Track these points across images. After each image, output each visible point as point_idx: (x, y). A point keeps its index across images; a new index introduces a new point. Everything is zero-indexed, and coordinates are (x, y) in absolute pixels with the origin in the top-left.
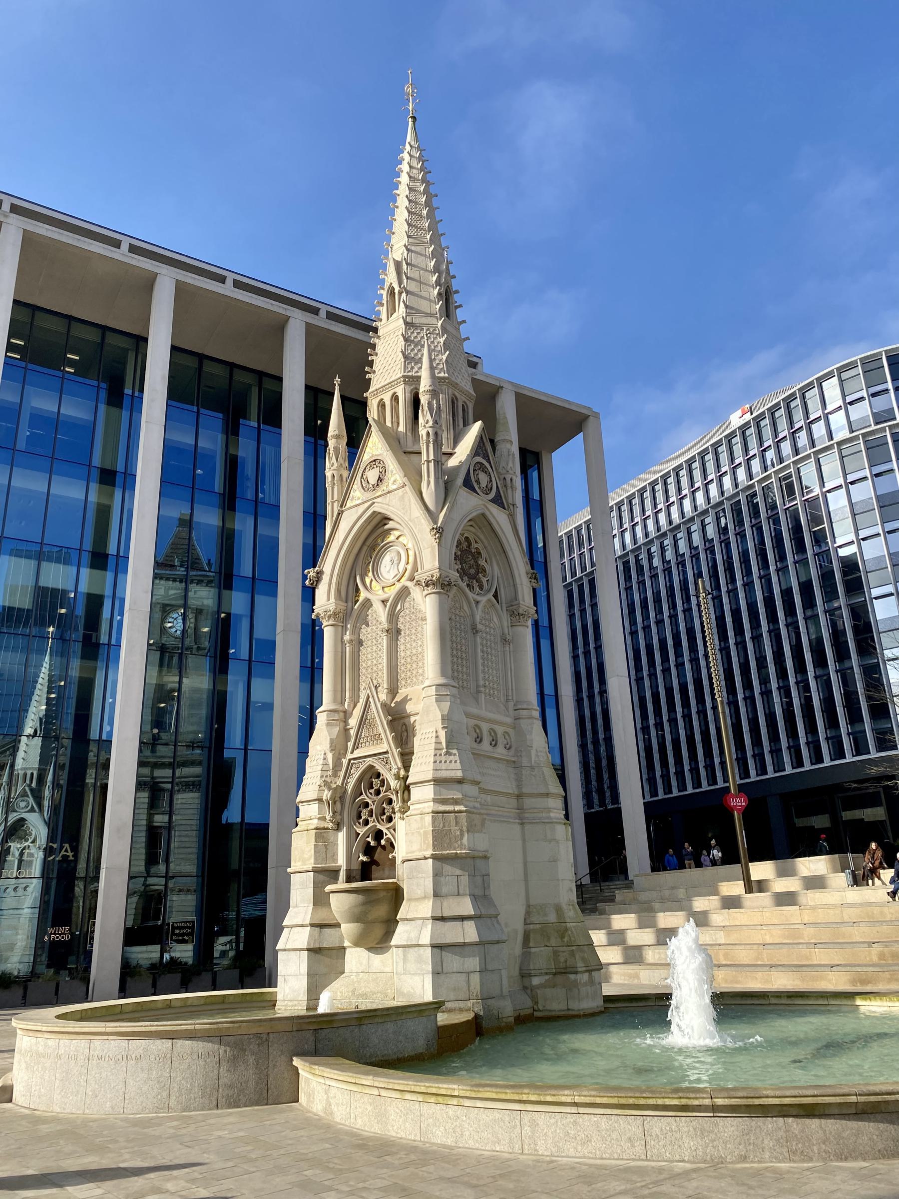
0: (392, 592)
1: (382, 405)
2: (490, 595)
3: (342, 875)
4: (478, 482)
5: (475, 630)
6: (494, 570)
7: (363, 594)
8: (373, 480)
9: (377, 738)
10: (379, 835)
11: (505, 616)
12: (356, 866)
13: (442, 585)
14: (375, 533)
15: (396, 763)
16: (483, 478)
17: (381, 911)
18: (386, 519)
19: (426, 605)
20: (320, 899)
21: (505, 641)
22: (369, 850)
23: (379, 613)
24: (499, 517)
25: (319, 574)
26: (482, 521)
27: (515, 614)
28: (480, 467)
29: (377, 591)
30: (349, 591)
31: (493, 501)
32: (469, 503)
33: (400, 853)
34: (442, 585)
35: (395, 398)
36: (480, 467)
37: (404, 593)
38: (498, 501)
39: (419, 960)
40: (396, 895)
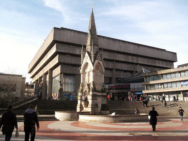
0: (88, 71)
5: (97, 75)
7: (86, 71)
8: (86, 58)
10: (87, 97)
13: (93, 71)
14: (87, 64)
16: (99, 58)
17: (86, 104)
18: (88, 63)
19: (91, 74)
21: (101, 76)
22: (86, 98)
23: (87, 73)
24: (101, 62)
25: (81, 68)
26: (99, 63)
27: (102, 73)
29: (87, 70)
31: (100, 60)
33: (88, 99)
34: (93, 71)
37: (90, 71)
40: (88, 102)
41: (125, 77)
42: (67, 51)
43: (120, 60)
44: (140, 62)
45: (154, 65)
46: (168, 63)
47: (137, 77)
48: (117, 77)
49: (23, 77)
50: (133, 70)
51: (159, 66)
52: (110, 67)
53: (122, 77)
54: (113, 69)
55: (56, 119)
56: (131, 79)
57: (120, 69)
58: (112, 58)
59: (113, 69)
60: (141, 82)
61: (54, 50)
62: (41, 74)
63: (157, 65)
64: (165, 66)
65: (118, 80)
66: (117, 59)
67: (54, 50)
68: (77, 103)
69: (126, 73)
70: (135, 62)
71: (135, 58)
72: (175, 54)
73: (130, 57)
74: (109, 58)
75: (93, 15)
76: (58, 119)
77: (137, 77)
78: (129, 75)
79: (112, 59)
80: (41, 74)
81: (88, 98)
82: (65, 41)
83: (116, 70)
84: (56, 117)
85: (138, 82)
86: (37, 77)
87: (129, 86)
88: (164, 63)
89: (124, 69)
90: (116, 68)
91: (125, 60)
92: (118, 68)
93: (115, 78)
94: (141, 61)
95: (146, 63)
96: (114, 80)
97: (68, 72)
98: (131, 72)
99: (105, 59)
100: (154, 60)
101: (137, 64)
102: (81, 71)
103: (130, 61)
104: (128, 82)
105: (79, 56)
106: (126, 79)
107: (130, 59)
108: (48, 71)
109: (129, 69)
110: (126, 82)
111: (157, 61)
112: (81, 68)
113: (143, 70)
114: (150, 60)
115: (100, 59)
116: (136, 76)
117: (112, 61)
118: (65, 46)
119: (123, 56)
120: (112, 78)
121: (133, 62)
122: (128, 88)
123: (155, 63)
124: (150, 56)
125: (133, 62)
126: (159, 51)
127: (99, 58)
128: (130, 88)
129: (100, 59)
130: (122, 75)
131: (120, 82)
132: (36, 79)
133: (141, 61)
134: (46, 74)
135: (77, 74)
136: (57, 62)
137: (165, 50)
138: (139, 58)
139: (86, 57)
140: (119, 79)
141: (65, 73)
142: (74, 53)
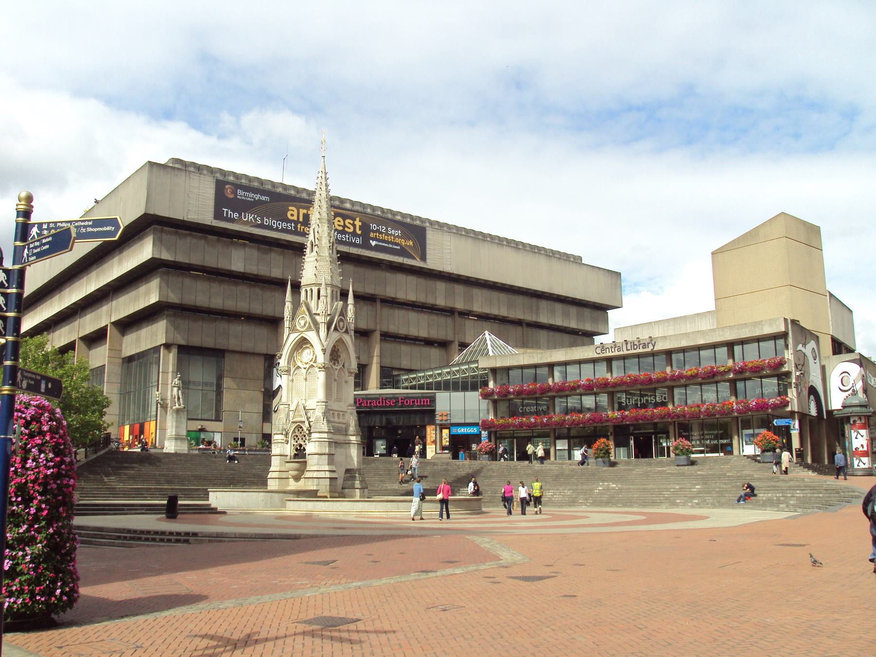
0: (308, 366)
6: (343, 355)
8: (302, 324)
13: (325, 368)
15: (307, 423)
16: (341, 324)
18: (305, 339)
22: (297, 450)
26: (340, 341)
32: (335, 336)
38: (347, 332)
42: (195, 259)
43: (401, 296)
44: (477, 308)
46: (587, 312)
47: (463, 367)
48: (388, 363)
54: (373, 331)
55: (216, 509)
56: (440, 374)
59: (373, 331)
60: (474, 388)
63: (543, 319)
66: (390, 292)
70: (460, 305)
71: (459, 288)
72: (618, 274)
73: (441, 286)
76: (219, 509)
77: (463, 367)
79: (373, 292)
81: (304, 449)
83: (386, 336)
84: (213, 506)
85: (465, 388)
87: (433, 400)
88: (573, 310)
89: (413, 332)
90: (385, 329)
91: (421, 298)
92: (392, 329)
94: (480, 302)
95: (503, 312)
97: (196, 341)
98: (444, 345)
100: (534, 300)
101: (464, 314)
103: (441, 302)
104: (429, 386)
107: (440, 294)
110: (421, 387)
111: (543, 304)
113: (488, 342)
116: (458, 365)
118: (191, 235)
119: (412, 280)
121: (450, 304)
122: (428, 414)
123: (538, 309)
125: (452, 305)
126: (556, 265)
127: (341, 324)
128: (434, 411)
133: (480, 302)
134: (96, 338)
135: (230, 348)
137: (576, 260)
138: (477, 292)
139: (302, 322)
142: (223, 265)
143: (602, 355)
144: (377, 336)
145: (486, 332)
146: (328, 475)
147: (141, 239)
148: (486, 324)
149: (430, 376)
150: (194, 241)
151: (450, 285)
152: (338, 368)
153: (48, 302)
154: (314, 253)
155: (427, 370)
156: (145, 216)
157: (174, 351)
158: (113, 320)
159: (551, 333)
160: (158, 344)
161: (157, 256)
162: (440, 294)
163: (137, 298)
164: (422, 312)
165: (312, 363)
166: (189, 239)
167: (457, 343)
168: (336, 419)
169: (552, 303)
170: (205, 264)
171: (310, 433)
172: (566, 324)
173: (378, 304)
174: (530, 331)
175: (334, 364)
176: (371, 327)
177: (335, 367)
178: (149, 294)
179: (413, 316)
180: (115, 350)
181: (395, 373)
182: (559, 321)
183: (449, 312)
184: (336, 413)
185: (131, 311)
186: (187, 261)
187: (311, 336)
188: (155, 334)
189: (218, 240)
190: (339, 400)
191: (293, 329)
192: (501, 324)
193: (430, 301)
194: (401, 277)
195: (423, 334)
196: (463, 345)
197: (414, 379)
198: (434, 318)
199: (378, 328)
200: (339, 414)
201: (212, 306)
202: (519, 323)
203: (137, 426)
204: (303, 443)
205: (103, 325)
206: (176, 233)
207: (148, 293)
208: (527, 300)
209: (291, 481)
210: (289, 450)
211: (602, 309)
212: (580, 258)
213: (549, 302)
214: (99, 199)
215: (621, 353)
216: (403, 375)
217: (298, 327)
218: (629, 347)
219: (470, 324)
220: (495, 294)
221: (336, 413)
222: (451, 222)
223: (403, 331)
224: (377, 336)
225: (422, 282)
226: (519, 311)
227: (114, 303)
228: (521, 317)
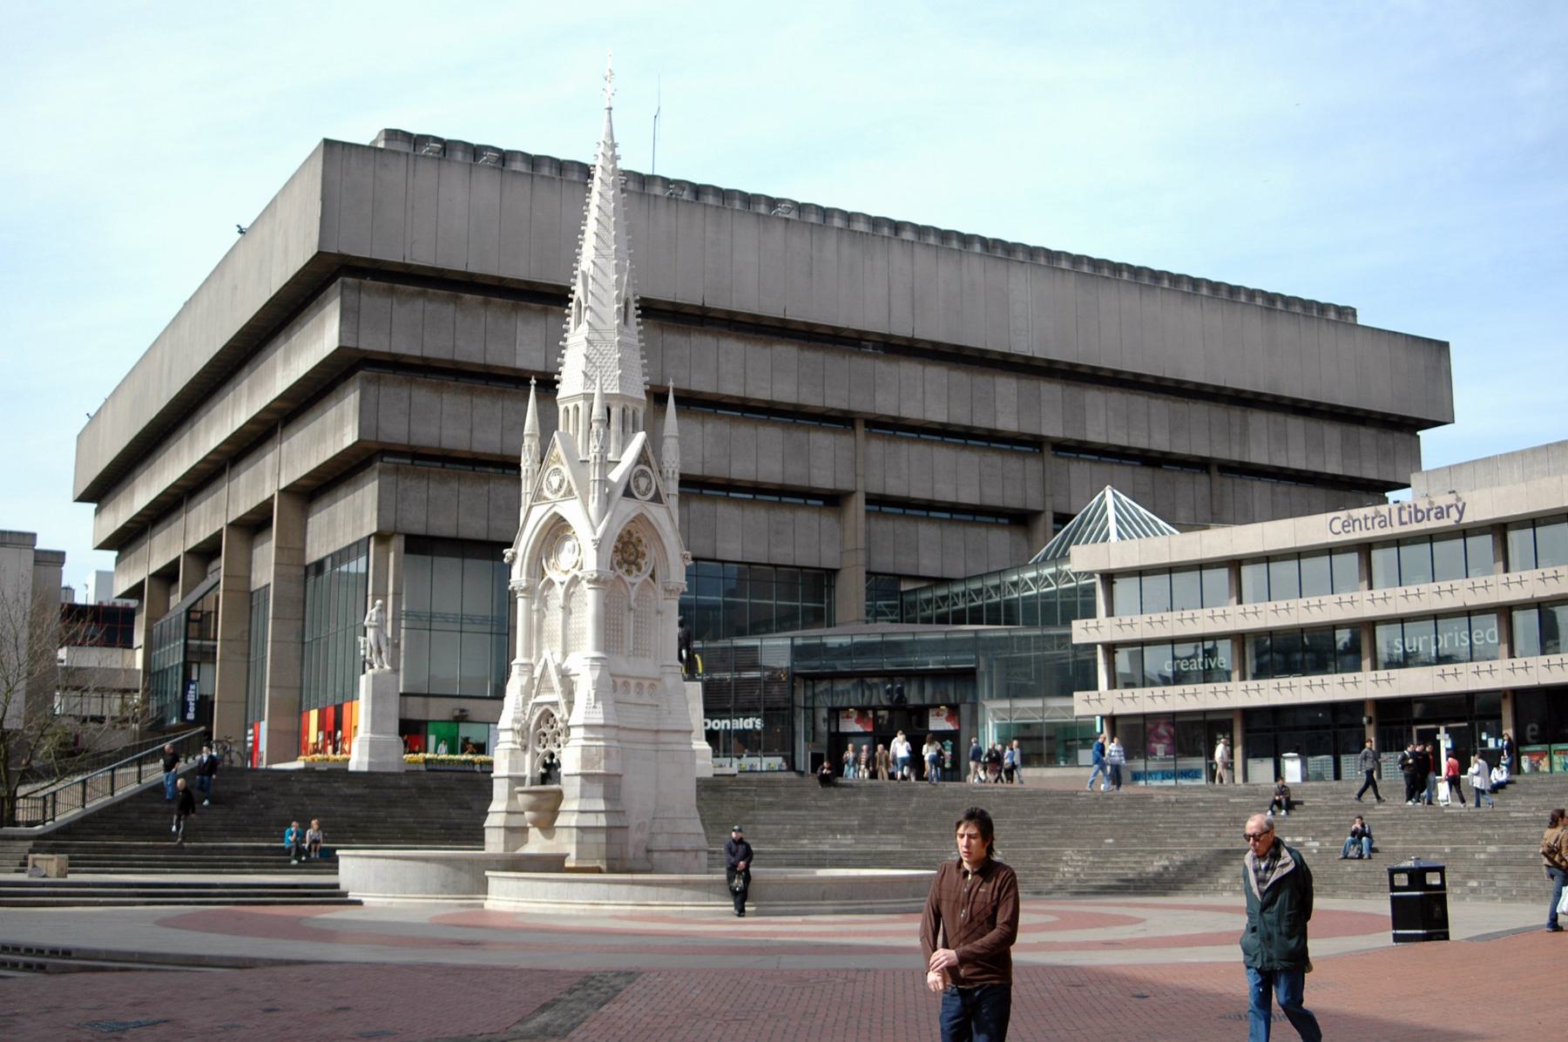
0: (567, 578)
1: (567, 410)
2: (647, 576)
3: (528, 781)
4: (637, 487)
8: (555, 485)
9: (551, 690)
10: (552, 756)
11: (660, 591)
12: (537, 775)
14: (557, 530)
15: (563, 708)
16: (643, 482)
17: (549, 805)
18: (562, 519)
19: (588, 601)
20: (512, 796)
22: (545, 765)
23: (559, 591)
24: (657, 513)
25: (515, 555)
26: (640, 519)
28: (643, 473)
29: (562, 566)
30: (537, 568)
32: (629, 508)
33: (564, 770)
35: (577, 408)
36: (643, 473)
37: (575, 581)
38: (657, 499)
39: (570, 835)
40: (559, 795)
41: (954, 569)
45: (1235, 455)
46: (1367, 435)
48: (885, 562)
49: (40, 545)
50: (1033, 505)
51: (1280, 461)
52: (823, 479)
53: (929, 565)
55: (345, 894)
56: (997, 588)
57: (914, 494)
58: (836, 400)
61: (320, 338)
62: (204, 520)
64: (1333, 467)
65: (890, 592)
66: (885, 405)
67: (320, 338)
68: (490, 798)
69: (976, 534)
70: (1053, 428)
71: (1051, 391)
72: (1444, 346)
73: (1006, 387)
74: (811, 398)
75: (614, 146)
76: (352, 896)
78: (1000, 540)
79: (844, 406)
80: (204, 520)
81: (559, 764)
82: (422, 255)
83: (879, 503)
84: (343, 888)
86: (164, 549)
88: (1332, 433)
89: (945, 492)
90: (876, 488)
91: (960, 416)
92: (895, 488)
93: (862, 571)
94: (1103, 419)
95: (1160, 442)
96: (851, 593)
97: (443, 526)
98: (1021, 520)
99: (692, 485)
100: (1236, 413)
102: (518, 577)
103: (1007, 422)
105: (509, 466)
106: (959, 589)
107: (1006, 405)
108: (266, 506)
109: (994, 498)
112: (520, 552)
113: (1111, 512)
114: (1199, 411)
115: (648, 489)
117: (842, 421)
119: (937, 374)
120: (833, 573)
121: (1029, 427)
124: (1194, 373)
126: (1286, 329)
127: (643, 482)
129: (648, 489)
130: (930, 550)
131: (905, 613)
132: (158, 563)
133: (1103, 419)
134: (254, 525)
136: (349, 436)
137: (1345, 314)
138: (1095, 398)
139: (555, 481)
140: (905, 586)
141: (418, 529)
143: (1344, 537)
144: (858, 506)
145: (1108, 491)
146: (602, 821)
147: (321, 306)
148: (1102, 469)
149: (979, 592)
150: (430, 307)
151: (1029, 385)
152: (639, 580)
153: (173, 449)
154: (584, 327)
155: (989, 574)
156: (319, 257)
157: (398, 544)
158: (283, 485)
159: (1282, 488)
160: (365, 534)
161: (351, 344)
162: (1006, 405)
163: (321, 438)
164: (965, 446)
165: (575, 571)
166: (419, 304)
167: (1049, 516)
168: (632, 697)
169: (1280, 418)
170: (458, 358)
171: (569, 728)
172: (1315, 465)
173: (861, 430)
174: (1228, 484)
175: (629, 572)
176: (844, 484)
177: (627, 579)
178: (337, 429)
179: (943, 456)
180: (292, 549)
181: (905, 586)
182: (1296, 460)
183: (1031, 444)
184: (633, 683)
185: (313, 465)
186: (417, 353)
187: (571, 510)
188: (353, 516)
189: (486, 304)
190: (639, 651)
191: (538, 497)
192: (1149, 468)
193: (982, 421)
194: (910, 370)
195: (969, 496)
196: (1062, 519)
197: (944, 598)
198: (994, 459)
199: (860, 486)
200: (639, 685)
201: (478, 448)
202: (1202, 465)
203: (331, 712)
204: (555, 750)
205: (267, 496)
206: (392, 292)
207: (339, 425)
208: (1218, 413)
209: (534, 832)
210: (529, 767)
211: (1409, 426)
212: (1353, 312)
213: (1273, 416)
214: (245, 226)
215: (1388, 531)
216: (921, 589)
217: (547, 493)
218: (1405, 518)
219: (1079, 470)
220: (1139, 401)
221: (633, 683)
222: (1032, 241)
223: (919, 492)
224: (858, 506)
225: (961, 378)
226: (1197, 434)
227: (285, 445)
228: (1204, 452)
